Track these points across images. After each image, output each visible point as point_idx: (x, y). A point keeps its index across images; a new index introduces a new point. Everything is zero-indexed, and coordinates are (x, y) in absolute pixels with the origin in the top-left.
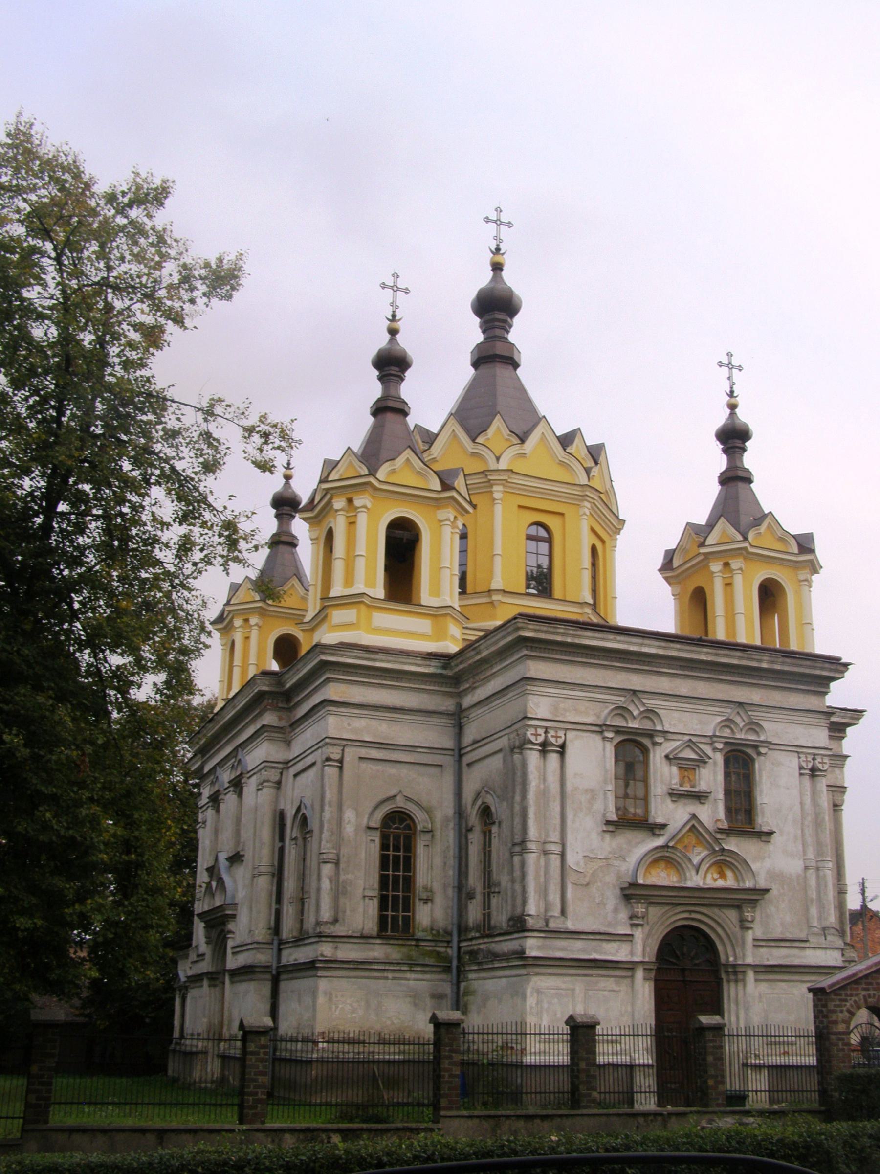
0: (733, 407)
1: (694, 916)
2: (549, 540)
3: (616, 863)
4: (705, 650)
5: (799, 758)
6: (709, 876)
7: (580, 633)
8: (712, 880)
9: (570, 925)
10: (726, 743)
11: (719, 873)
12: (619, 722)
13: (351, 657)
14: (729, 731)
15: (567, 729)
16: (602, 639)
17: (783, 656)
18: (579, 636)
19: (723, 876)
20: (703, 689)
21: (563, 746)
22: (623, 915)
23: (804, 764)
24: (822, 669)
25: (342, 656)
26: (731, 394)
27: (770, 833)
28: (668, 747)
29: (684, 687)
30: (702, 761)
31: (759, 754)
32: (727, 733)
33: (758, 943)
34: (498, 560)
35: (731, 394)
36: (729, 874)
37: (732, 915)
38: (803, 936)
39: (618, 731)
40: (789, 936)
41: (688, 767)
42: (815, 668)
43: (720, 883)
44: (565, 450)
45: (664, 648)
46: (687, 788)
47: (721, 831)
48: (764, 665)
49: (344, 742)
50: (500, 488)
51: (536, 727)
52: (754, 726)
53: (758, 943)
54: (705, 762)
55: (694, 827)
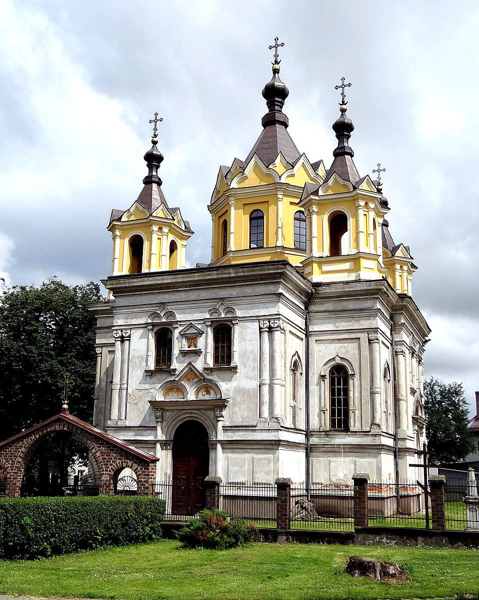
0: (343, 111)
1: (192, 415)
2: (263, 217)
3: (151, 391)
4: (196, 274)
5: (259, 322)
6: (200, 393)
7: (131, 280)
8: (203, 396)
9: (128, 424)
10: (212, 322)
11: (206, 392)
12: (157, 321)
13: (99, 307)
14: (217, 314)
15: (131, 328)
16: (143, 281)
17: (241, 268)
18: (132, 282)
19: (208, 393)
20: (204, 294)
21: (129, 337)
22: (153, 417)
23: (262, 326)
24: (269, 270)
25: (96, 307)
26: (343, 103)
27: (236, 368)
28: (181, 329)
29: (193, 295)
30: (200, 333)
31: (233, 324)
32: (215, 316)
33: (226, 429)
34: (232, 236)
35: (343, 103)
36: (212, 392)
37: (210, 414)
38: (254, 424)
39: (153, 325)
40: (245, 424)
41: (192, 339)
42: (264, 270)
43: (207, 397)
44: (267, 167)
45: (175, 278)
46: (193, 348)
47: (205, 369)
48: (232, 275)
49: (102, 345)
50: (232, 198)
51: (117, 330)
52: (230, 310)
53: (226, 429)
54: (202, 334)
55: (191, 368)
